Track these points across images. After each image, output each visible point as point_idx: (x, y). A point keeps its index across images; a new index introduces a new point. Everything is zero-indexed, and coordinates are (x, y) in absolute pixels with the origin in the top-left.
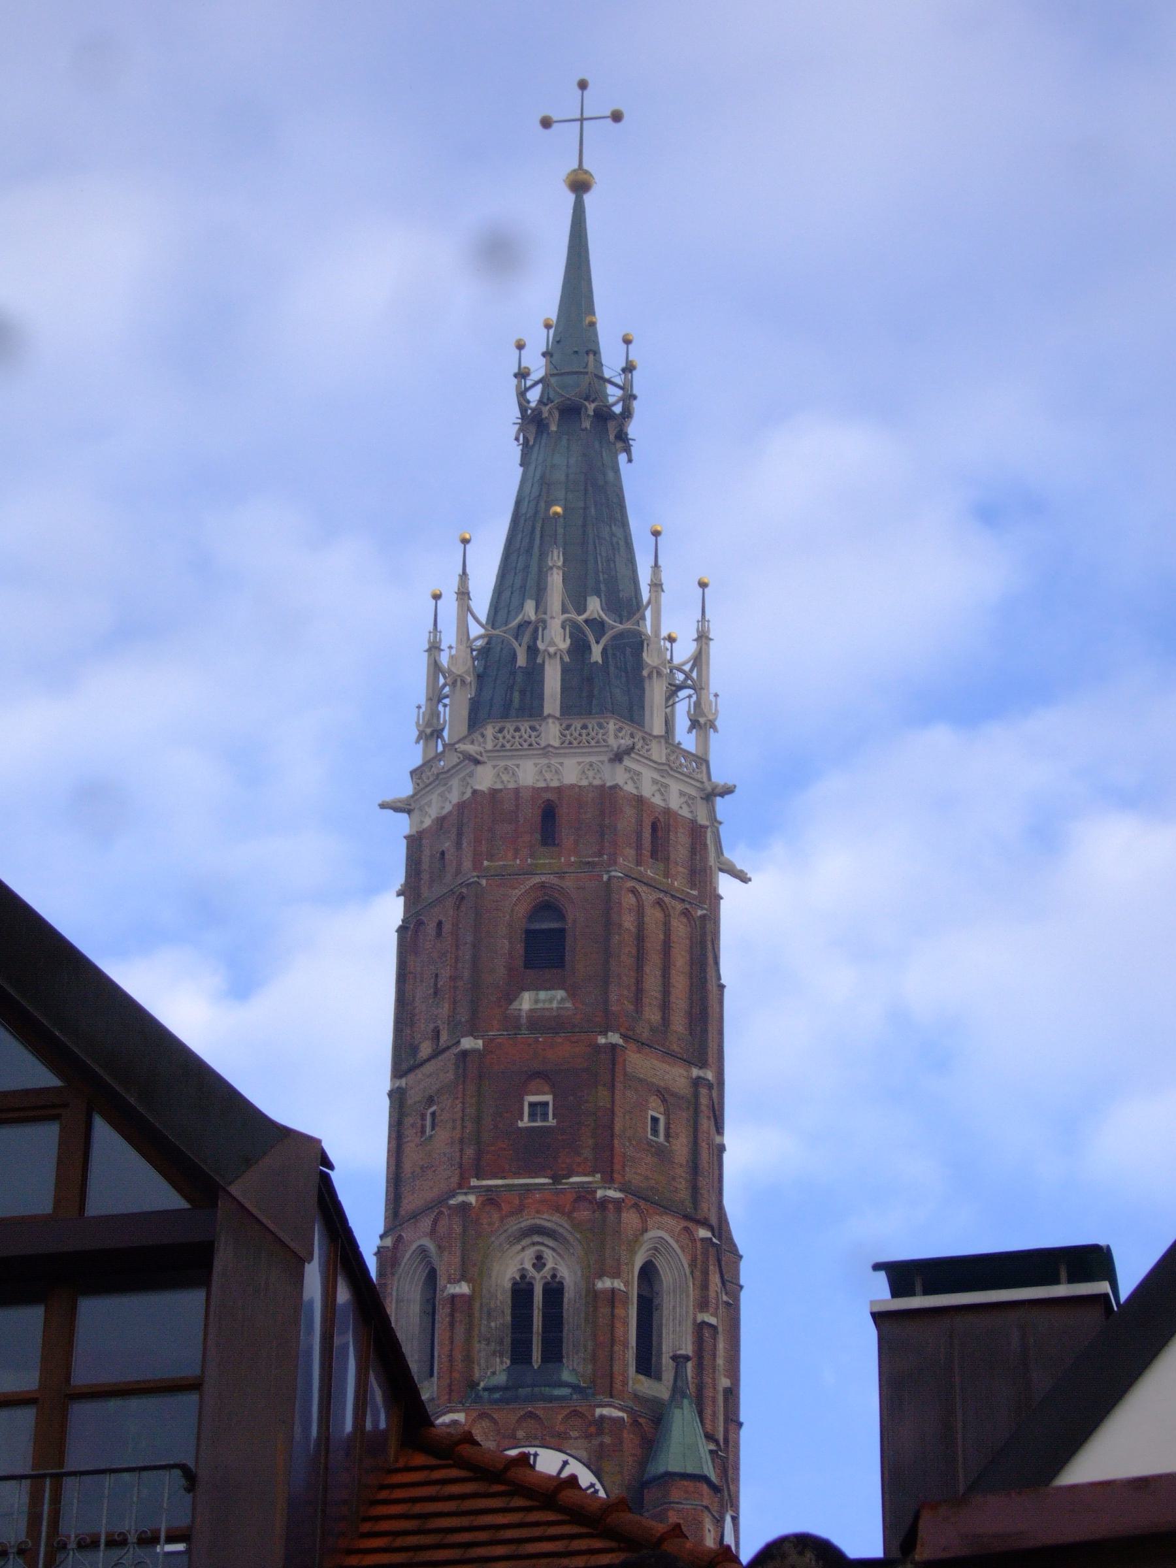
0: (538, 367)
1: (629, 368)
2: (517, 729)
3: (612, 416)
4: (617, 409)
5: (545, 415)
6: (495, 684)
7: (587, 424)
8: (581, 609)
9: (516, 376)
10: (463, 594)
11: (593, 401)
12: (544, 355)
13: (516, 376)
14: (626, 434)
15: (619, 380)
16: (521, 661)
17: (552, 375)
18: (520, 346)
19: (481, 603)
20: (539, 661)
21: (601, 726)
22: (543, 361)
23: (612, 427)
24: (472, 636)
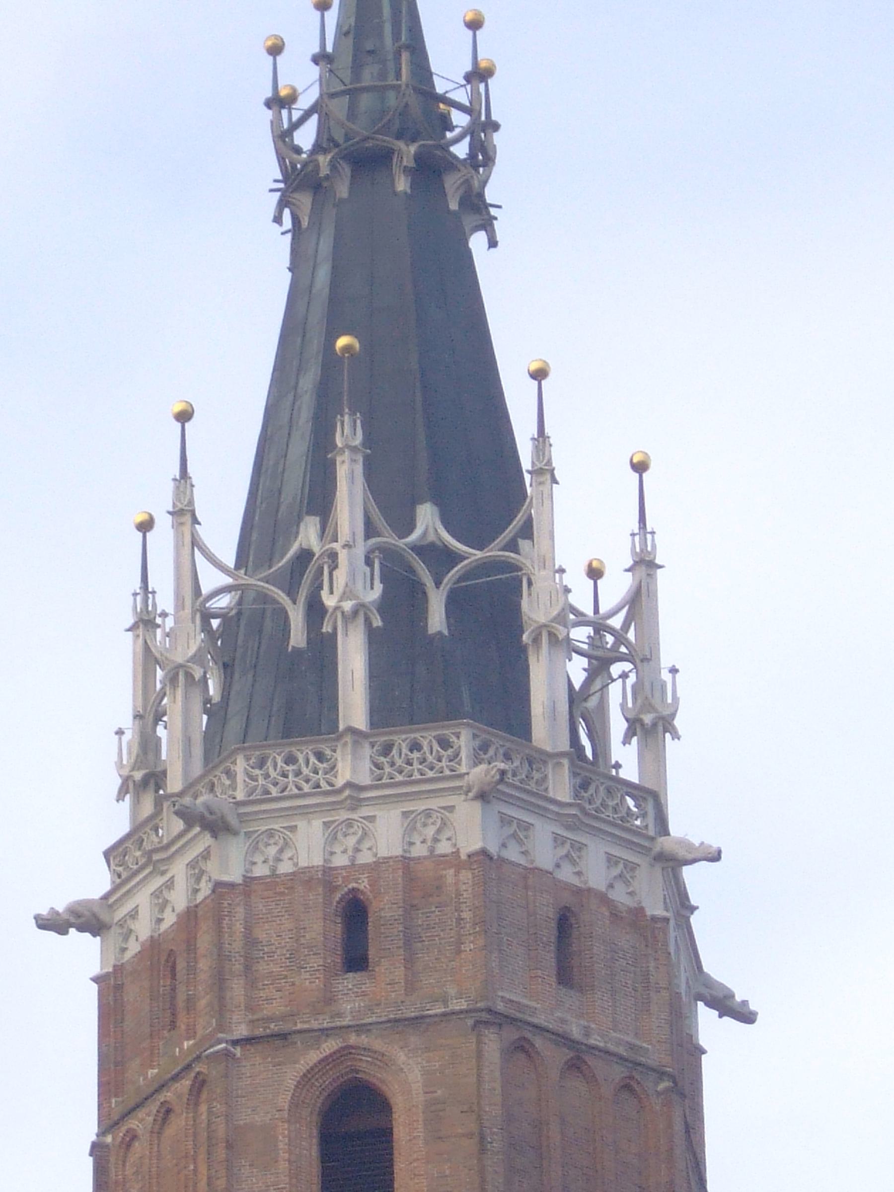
0: (305, 80)
1: (479, 75)
2: (290, 760)
3: (452, 163)
4: (461, 150)
5: (324, 171)
6: (251, 675)
7: (402, 184)
8: (406, 525)
9: (269, 104)
10: (184, 513)
11: (413, 140)
12: (316, 60)
13: (269, 104)
14: (481, 195)
15: (461, 96)
16: (298, 637)
17: (333, 96)
18: (275, 50)
19: (222, 524)
20: (327, 628)
21: (444, 743)
22: (314, 72)
23: (451, 182)
24: (205, 590)
